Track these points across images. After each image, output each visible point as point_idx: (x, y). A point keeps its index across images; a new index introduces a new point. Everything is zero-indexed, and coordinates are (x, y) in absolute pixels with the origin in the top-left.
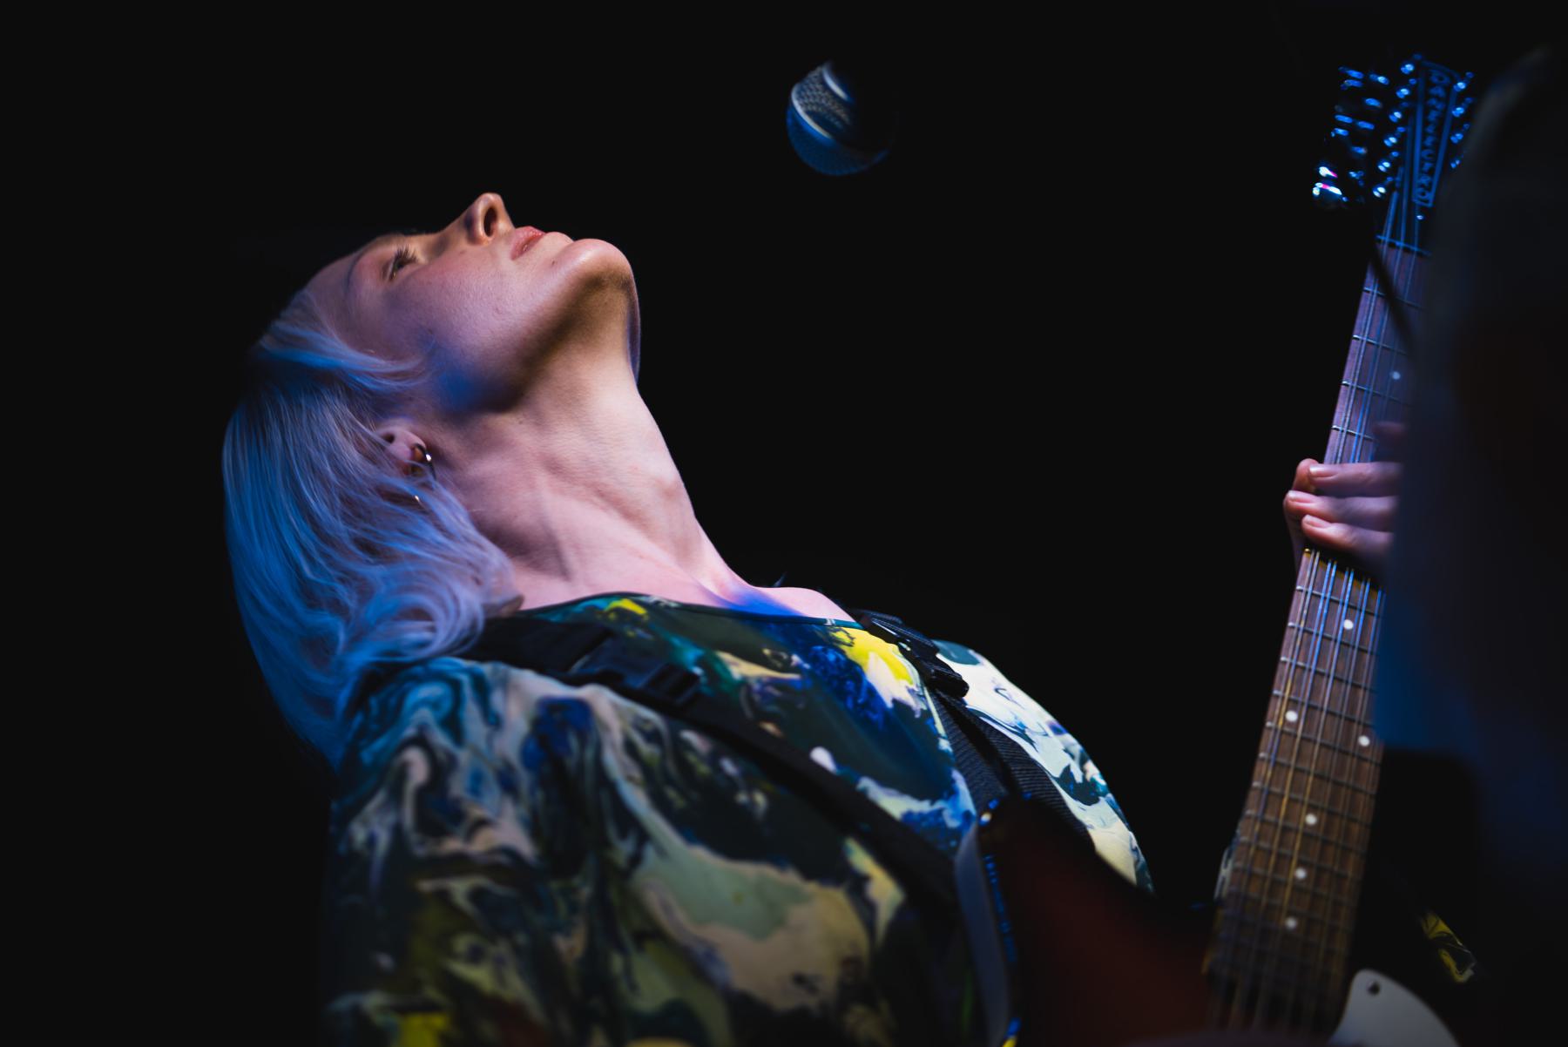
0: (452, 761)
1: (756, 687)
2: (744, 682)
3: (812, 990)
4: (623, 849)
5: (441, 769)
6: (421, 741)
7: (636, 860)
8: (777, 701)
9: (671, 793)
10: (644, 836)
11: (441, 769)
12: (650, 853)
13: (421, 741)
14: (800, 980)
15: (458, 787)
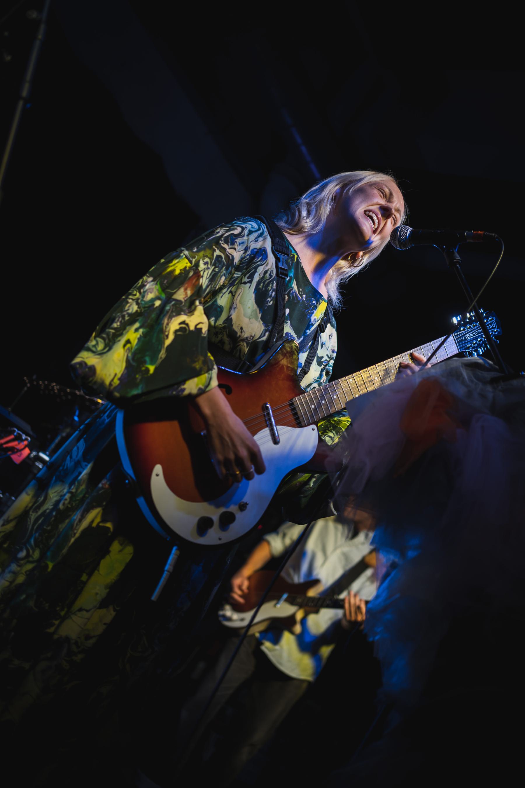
0: (244, 236)
1: (293, 291)
2: (293, 288)
3: (241, 332)
4: (245, 279)
5: (239, 235)
6: (243, 229)
7: (245, 283)
8: (293, 296)
9: (262, 284)
10: (250, 282)
11: (239, 235)
12: (248, 285)
13: (243, 229)
14: (242, 328)
15: (238, 240)
